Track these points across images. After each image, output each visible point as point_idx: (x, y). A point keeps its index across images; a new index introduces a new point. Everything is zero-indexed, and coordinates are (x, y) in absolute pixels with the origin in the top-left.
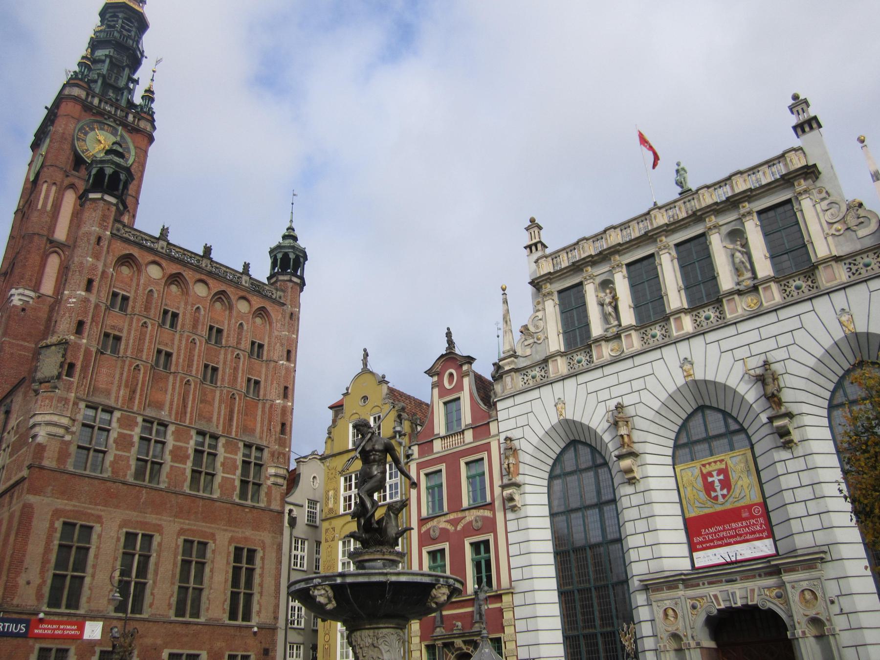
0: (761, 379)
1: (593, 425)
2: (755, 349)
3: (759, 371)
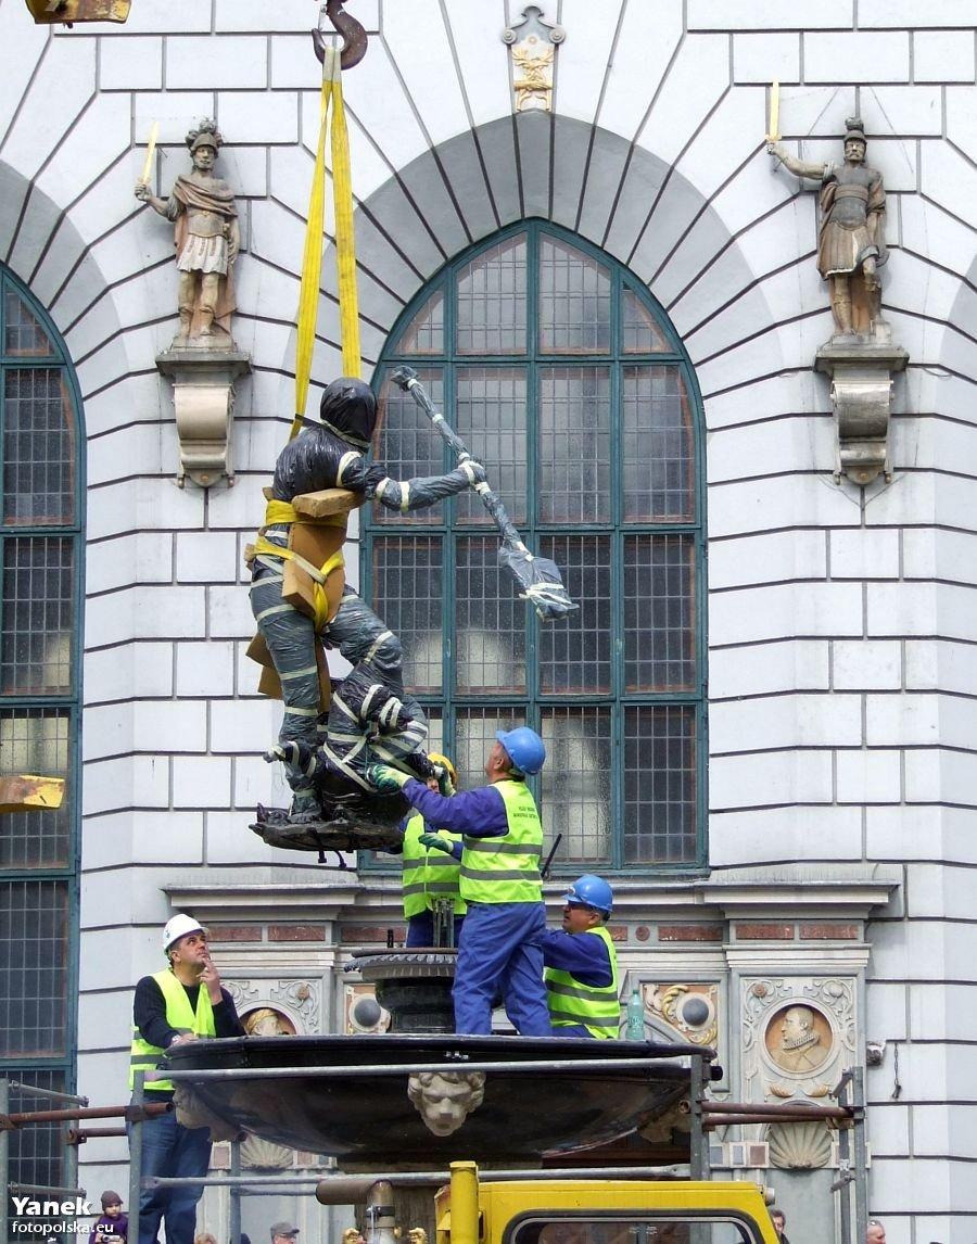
0: (818, 188)
1: (57, 187)
2: (827, 58)
3: (823, 156)
